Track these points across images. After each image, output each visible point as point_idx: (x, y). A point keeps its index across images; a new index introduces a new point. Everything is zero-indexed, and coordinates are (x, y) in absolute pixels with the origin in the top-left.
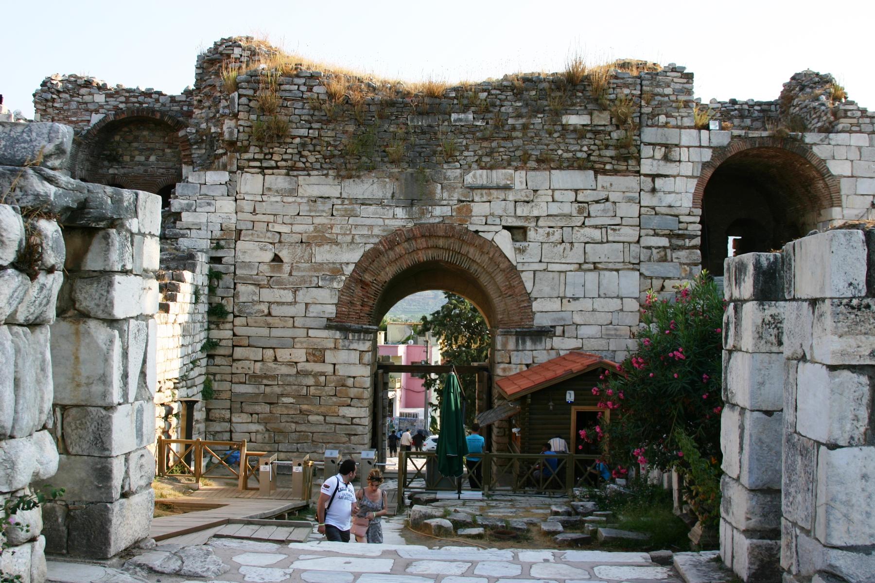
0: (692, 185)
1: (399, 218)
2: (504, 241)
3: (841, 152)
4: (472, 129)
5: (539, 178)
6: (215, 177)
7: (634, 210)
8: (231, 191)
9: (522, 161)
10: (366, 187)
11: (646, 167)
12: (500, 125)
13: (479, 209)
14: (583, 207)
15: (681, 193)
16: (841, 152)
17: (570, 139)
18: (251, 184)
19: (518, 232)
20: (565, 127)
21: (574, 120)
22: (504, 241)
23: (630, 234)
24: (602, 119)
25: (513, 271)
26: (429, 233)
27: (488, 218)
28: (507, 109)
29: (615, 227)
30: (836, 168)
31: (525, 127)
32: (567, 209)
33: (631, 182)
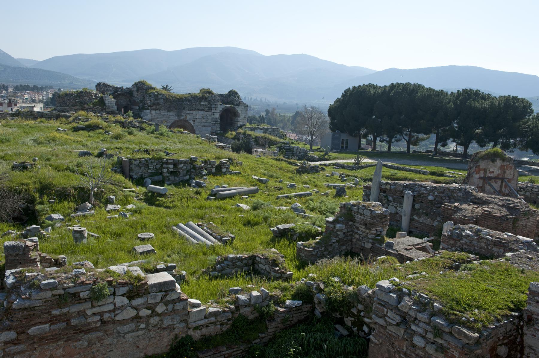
1: (176, 118)
2: (192, 122)
5: (197, 112)
6: (147, 111)
7: (210, 117)
8: (150, 113)
10: (172, 113)
11: (212, 111)
13: (188, 117)
14: (203, 117)
15: (217, 115)
18: (154, 112)
19: (194, 121)
21: (202, 103)
22: (192, 122)
23: (210, 121)
24: (207, 103)
25: (193, 127)
26: (181, 120)
27: (189, 118)
30: (239, 112)
33: (210, 113)
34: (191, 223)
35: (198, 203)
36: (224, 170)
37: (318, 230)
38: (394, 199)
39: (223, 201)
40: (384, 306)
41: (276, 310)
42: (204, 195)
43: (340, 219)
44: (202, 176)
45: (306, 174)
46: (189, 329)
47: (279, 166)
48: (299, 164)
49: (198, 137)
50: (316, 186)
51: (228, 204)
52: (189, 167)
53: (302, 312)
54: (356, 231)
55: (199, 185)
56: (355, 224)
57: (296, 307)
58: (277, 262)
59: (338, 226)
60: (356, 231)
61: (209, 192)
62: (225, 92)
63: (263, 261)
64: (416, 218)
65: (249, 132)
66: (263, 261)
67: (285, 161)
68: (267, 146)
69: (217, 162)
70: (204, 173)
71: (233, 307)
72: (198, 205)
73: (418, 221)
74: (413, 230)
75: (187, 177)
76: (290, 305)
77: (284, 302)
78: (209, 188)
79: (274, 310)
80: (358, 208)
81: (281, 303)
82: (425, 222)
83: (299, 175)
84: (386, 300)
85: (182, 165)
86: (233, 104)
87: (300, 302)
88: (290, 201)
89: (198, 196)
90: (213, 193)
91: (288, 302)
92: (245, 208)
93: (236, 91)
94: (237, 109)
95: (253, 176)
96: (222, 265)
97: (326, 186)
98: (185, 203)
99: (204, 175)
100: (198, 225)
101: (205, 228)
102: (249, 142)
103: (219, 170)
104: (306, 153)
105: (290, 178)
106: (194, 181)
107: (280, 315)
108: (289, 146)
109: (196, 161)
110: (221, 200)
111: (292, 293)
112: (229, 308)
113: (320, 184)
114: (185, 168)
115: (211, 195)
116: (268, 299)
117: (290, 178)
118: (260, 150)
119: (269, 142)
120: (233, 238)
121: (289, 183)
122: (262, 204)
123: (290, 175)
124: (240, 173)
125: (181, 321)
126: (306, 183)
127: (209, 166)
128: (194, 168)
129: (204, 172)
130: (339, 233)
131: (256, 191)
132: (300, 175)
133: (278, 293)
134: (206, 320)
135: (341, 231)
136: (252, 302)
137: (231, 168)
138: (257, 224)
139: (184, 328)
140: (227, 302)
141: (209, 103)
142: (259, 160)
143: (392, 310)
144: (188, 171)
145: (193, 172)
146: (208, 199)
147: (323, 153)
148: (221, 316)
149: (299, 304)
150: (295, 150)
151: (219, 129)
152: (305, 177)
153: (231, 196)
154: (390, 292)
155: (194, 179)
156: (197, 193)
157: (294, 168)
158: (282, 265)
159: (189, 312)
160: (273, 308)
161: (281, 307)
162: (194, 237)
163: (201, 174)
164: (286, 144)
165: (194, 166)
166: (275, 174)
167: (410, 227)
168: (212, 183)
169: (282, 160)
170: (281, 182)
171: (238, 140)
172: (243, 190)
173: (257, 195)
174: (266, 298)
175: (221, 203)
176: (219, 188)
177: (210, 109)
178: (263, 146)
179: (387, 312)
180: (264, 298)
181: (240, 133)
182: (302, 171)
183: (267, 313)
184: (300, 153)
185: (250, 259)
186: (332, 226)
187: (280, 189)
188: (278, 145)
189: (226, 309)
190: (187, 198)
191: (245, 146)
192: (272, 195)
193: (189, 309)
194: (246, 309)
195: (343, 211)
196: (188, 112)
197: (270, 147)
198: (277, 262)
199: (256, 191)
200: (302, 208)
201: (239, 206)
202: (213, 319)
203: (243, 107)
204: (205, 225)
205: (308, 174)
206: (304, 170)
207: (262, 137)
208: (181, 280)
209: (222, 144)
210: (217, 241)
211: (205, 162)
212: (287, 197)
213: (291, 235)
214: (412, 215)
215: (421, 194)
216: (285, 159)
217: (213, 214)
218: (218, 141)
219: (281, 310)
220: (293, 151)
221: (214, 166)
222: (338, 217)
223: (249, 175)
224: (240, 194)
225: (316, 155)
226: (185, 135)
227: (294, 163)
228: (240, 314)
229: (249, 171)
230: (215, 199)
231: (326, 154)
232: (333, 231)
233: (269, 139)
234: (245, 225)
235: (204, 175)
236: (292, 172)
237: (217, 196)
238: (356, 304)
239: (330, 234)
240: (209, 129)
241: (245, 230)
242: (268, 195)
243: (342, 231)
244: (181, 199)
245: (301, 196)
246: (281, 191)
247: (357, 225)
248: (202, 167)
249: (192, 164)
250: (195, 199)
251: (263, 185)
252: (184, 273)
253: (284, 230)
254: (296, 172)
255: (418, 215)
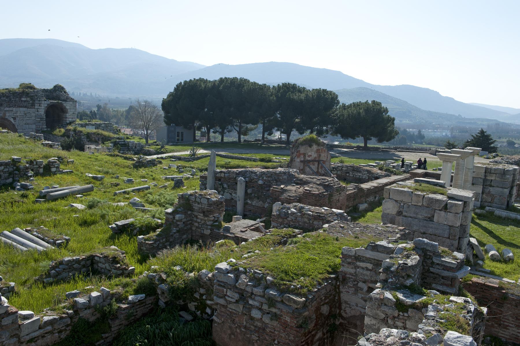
0: (44, 110)
2: (12, 120)
3: (68, 105)
4: (5, 101)
5: (18, 109)
9: (15, 106)
12: (10, 100)
13: (7, 114)
14: (25, 114)
15: (42, 112)
16: (68, 105)
17: (23, 102)
19: (14, 119)
20: (22, 101)
21: (23, 99)
22: (12, 120)
23: (34, 118)
24: (28, 99)
25: (14, 125)
28: (12, 97)
29: (31, 117)
30: (67, 107)
31: (15, 100)
32: (23, 114)
33: (34, 110)
34: (18, 229)
35: (25, 207)
36: (54, 170)
37: (158, 222)
38: (228, 186)
39: (54, 203)
40: (224, 287)
41: (119, 307)
42: (32, 198)
43: (179, 210)
44: (28, 178)
45: (143, 168)
46: (22, 343)
47: (115, 162)
48: (135, 159)
49: (20, 136)
50: (154, 179)
51: (61, 205)
52: (11, 169)
53: (146, 305)
54: (195, 219)
55: (24, 187)
56: (193, 213)
57: (139, 301)
58: (117, 259)
59: (177, 217)
60: (195, 219)
61: (37, 195)
62: (50, 87)
63: (102, 260)
64: (249, 202)
65: (79, 129)
66: (102, 260)
67: (121, 156)
68: (100, 142)
69: (45, 162)
70: (30, 174)
71: (71, 311)
72: (25, 209)
73: (251, 205)
74: (248, 213)
75: (10, 180)
76: (133, 300)
77: (127, 298)
78: (37, 189)
79: (116, 307)
80: (196, 197)
81: (124, 299)
82: (257, 205)
83: (136, 170)
84: (225, 281)
85: (3, 167)
86: (59, 100)
87: (143, 295)
88: (128, 196)
89: (25, 199)
90: (42, 195)
91: (130, 298)
92: (79, 208)
93: (62, 85)
94: (65, 105)
95: (87, 174)
96: (57, 269)
97: (164, 178)
98: (9, 208)
99: (31, 176)
100: (27, 231)
101: (35, 233)
102: (80, 139)
103: (47, 170)
104: (142, 147)
105: (127, 173)
106: (19, 184)
107: (123, 312)
108: (124, 141)
109: (19, 162)
110: (52, 201)
111: (134, 288)
112: (67, 313)
113: (157, 177)
114: (6, 170)
115: (40, 197)
116: (109, 298)
117: (127, 173)
118: (93, 147)
119: (103, 138)
120: (68, 241)
121: (126, 178)
122: (99, 202)
123: (127, 170)
124: (72, 172)
125: (12, 337)
126: (144, 177)
127: (35, 166)
128: (18, 169)
129: (31, 173)
130: (178, 223)
131: (91, 189)
132: (137, 169)
133: (120, 289)
134: (42, 331)
135: (180, 221)
136: (93, 303)
137: (62, 167)
138: (94, 223)
139: (15, 343)
140: (64, 308)
141: (32, 99)
142: (92, 157)
143: (230, 289)
144: (10, 173)
145: (16, 174)
146: (37, 201)
147: (159, 147)
148: (58, 323)
149: (142, 297)
150: (130, 145)
151: (45, 127)
152: (143, 171)
153: (63, 197)
154: (228, 273)
155: (18, 181)
156: (24, 196)
157: (130, 162)
158: (123, 262)
159: (20, 325)
160: (115, 306)
161: (124, 304)
162: (23, 244)
163: (27, 175)
164: (121, 139)
165: (17, 167)
166: (110, 170)
167: (244, 211)
168: (40, 184)
169: (117, 156)
170: (117, 178)
171: (68, 137)
172: (76, 189)
173: (92, 193)
174: (107, 297)
175: (52, 204)
176: (49, 188)
177: (33, 105)
178: (96, 142)
179: (227, 292)
180: (105, 297)
181: (70, 130)
182: (139, 165)
183: (110, 312)
184: (136, 147)
185: (88, 260)
186: (171, 217)
187: (117, 185)
188: (112, 141)
189: (64, 315)
190: (12, 203)
191: (76, 143)
192: (109, 192)
193: (20, 322)
194: (86, 311)
195: (181, 201)
196: (7, 109)
197: (103, 143)
198: (117, 259)
199: (91, 189)
200: (141, 202)
201: (73, 206)
202: (49, 328)
203: (71, 103)
204: (35, 230)
205: (145, 168)
206: (141, 164)
207: (94, 133)
208: (9, 292)
209: (50, 142)
210: (49, 245)
211: (31, 162)
212: (125, 193)
213: (131, 230)
214: (245, 199)
215: (252, 180)
216: (120, 154)
217: (43, 217)
218: (45, 140)
219: (124, 306)
220: (129, 146)
221: (42, 166)
222: (177, 208)
223: (82, 173)
224: (73, 194)
225: (152, 149)
226: (5, 134)
227: (130, 158)
228: (80, 318)
229: (82, 169)
230: (45, 202)
231: (162, 147)
232: (173, 221)
233: (102, 135)
234: (81, 225)
235: (31, 176)
236: (128, 167)
237: (47, 198)
238: (198, 289)
239: (171, 224)
240: (34, 126)
241: (81, 230)
242: (105, 192)
243: (181, 221)
244: (4, 204)
245: (139, 190)
246: (118, 187)
247: (196, 213)
248: (27, 168)
249: (15, 166)
250: (21, 203)
251: (98, 182)
252: (12, 284)
253: (123, 226)
254: (132, 167)
255: (251, 199)
